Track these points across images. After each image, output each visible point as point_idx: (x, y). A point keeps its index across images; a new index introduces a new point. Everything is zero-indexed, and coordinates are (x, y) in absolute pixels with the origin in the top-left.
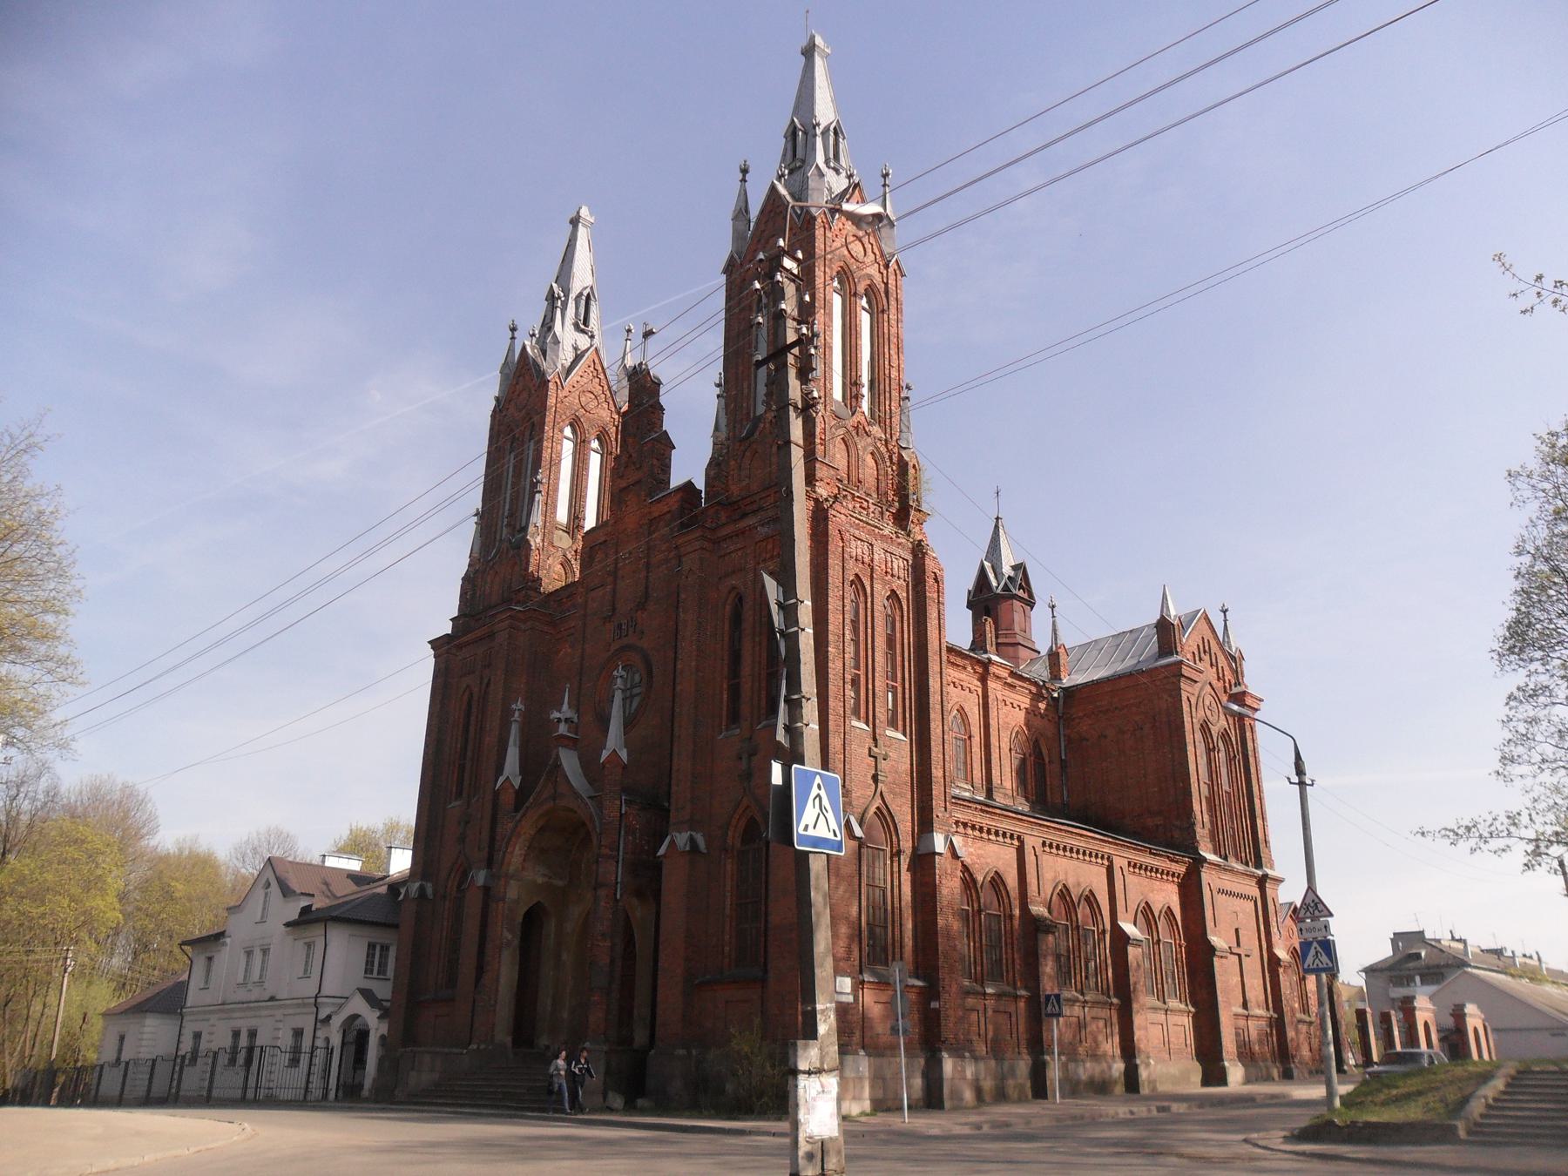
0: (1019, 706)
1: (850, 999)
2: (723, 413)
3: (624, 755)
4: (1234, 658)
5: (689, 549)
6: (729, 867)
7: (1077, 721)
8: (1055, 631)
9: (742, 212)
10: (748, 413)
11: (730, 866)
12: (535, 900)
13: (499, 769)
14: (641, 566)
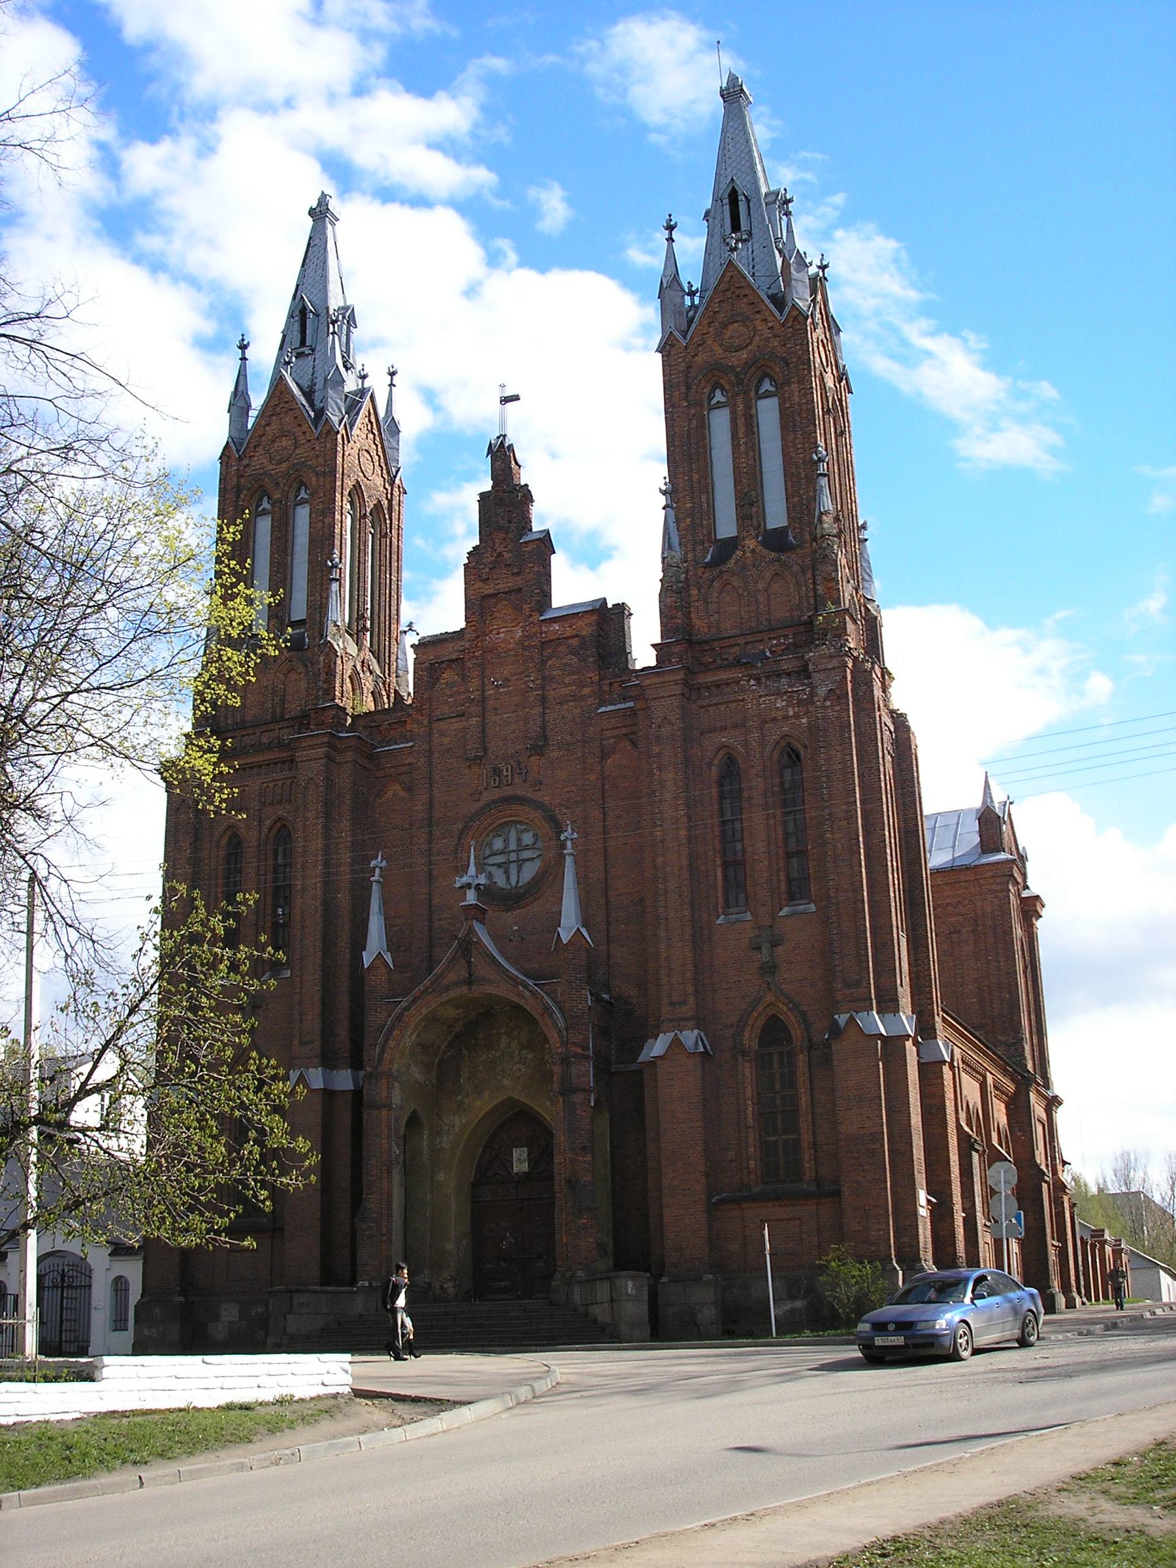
2: (673, 527)
6: (748, 1072)
11: (748, 1071)
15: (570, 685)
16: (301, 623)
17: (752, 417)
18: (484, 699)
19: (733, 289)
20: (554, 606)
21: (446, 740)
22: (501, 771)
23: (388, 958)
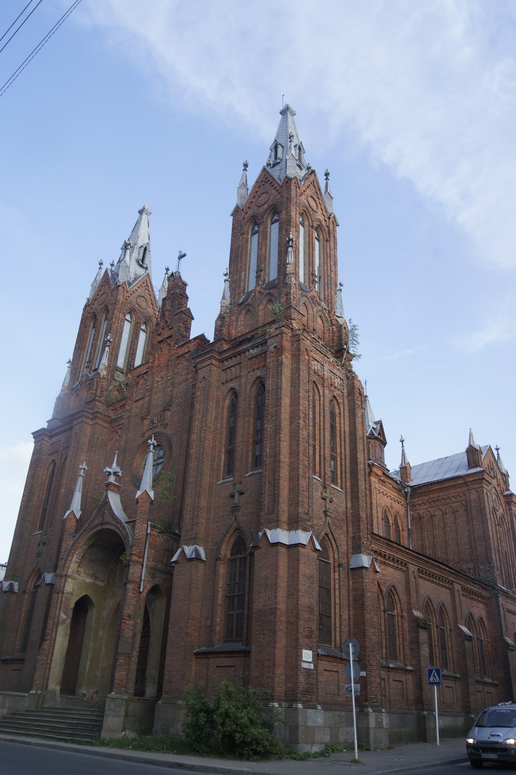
0: (386, 494)
1: (312, 666)
3: (152, 494)
4: (504, 475)
5: (204, 364)
7: (418, 506)
8: (403, 455)
9: (244, 185)
10: (244, 290)
12: (84, 594)
13: (67, 505)
14: (168, 384)
17: (266, 232)
18: (152, 388)
22: (154, 420)
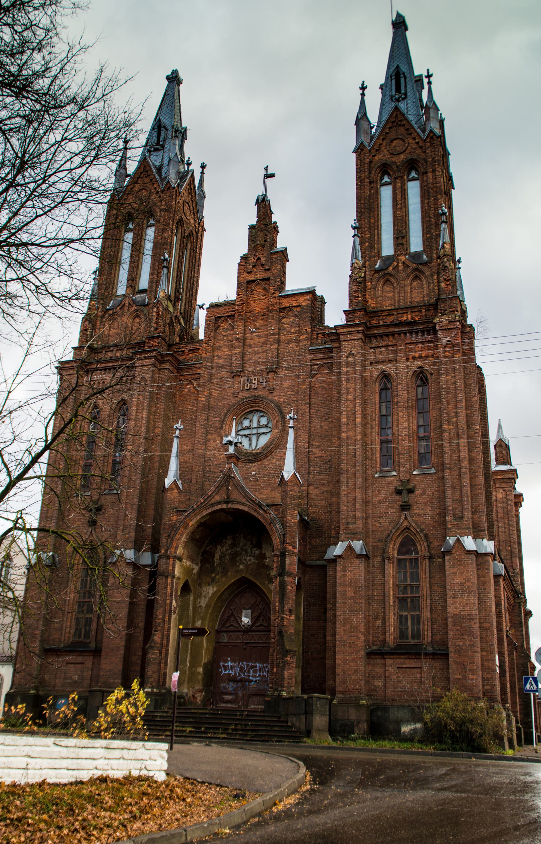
15: (294, 333)
16: (144, 291)
18: (245, 339)
19: (397, 121)
20: (287, 288)
21: (221, 361)
22: (251, 380)
23: (179, 483)
